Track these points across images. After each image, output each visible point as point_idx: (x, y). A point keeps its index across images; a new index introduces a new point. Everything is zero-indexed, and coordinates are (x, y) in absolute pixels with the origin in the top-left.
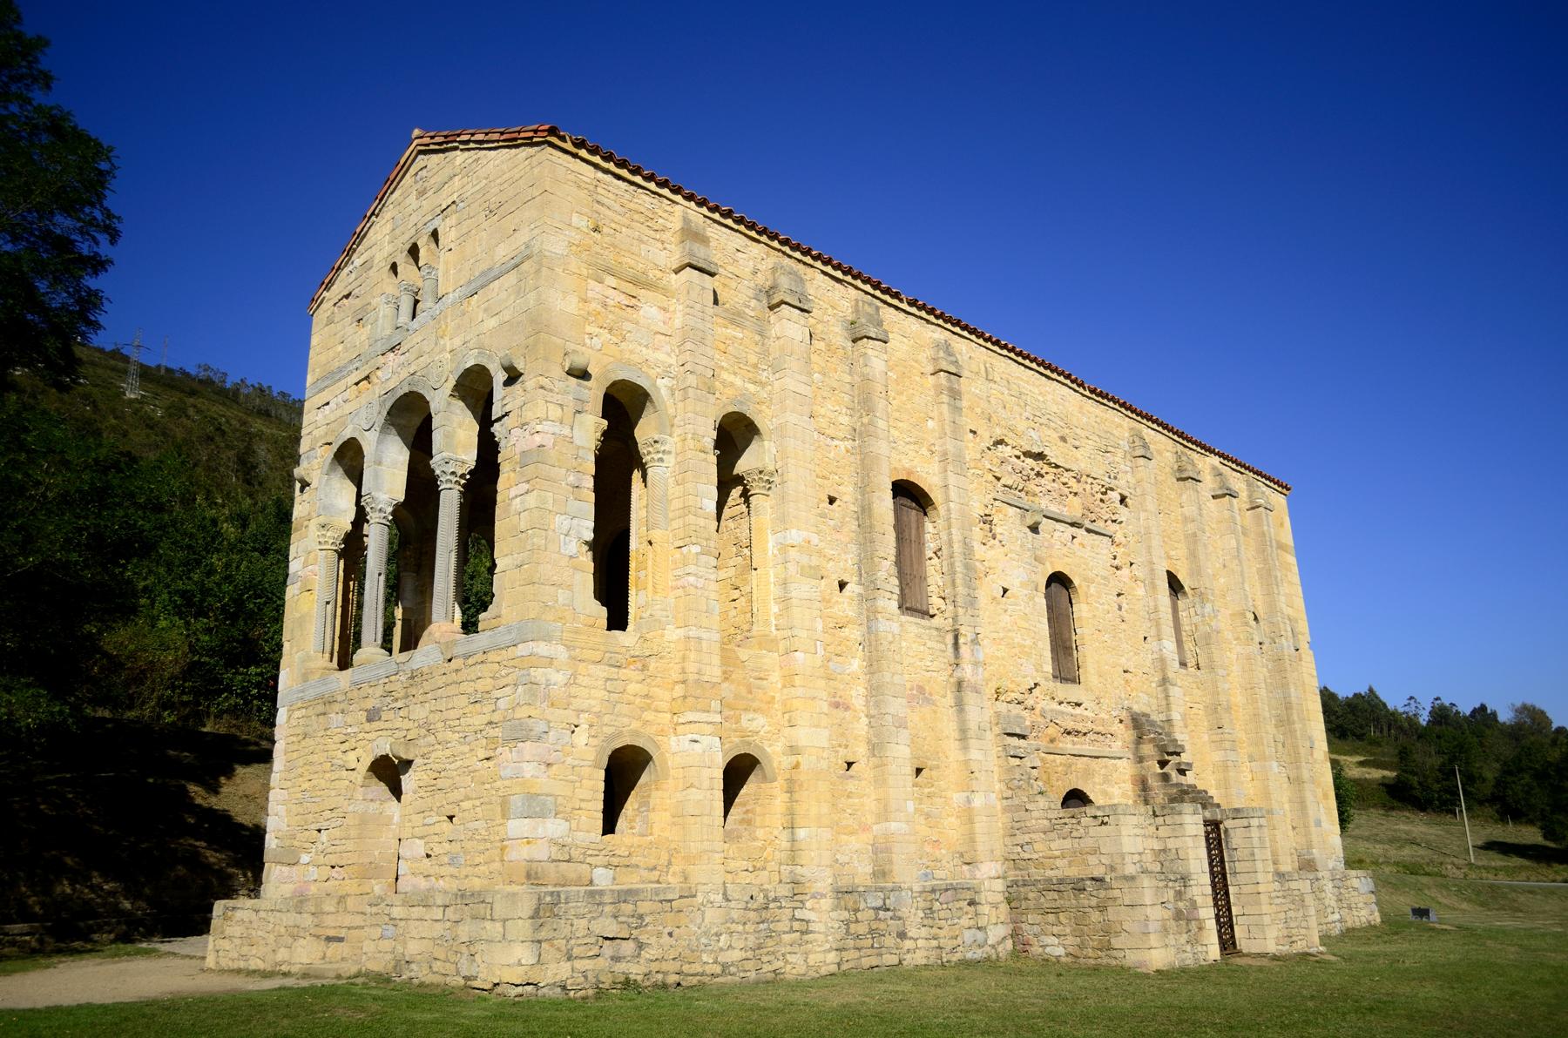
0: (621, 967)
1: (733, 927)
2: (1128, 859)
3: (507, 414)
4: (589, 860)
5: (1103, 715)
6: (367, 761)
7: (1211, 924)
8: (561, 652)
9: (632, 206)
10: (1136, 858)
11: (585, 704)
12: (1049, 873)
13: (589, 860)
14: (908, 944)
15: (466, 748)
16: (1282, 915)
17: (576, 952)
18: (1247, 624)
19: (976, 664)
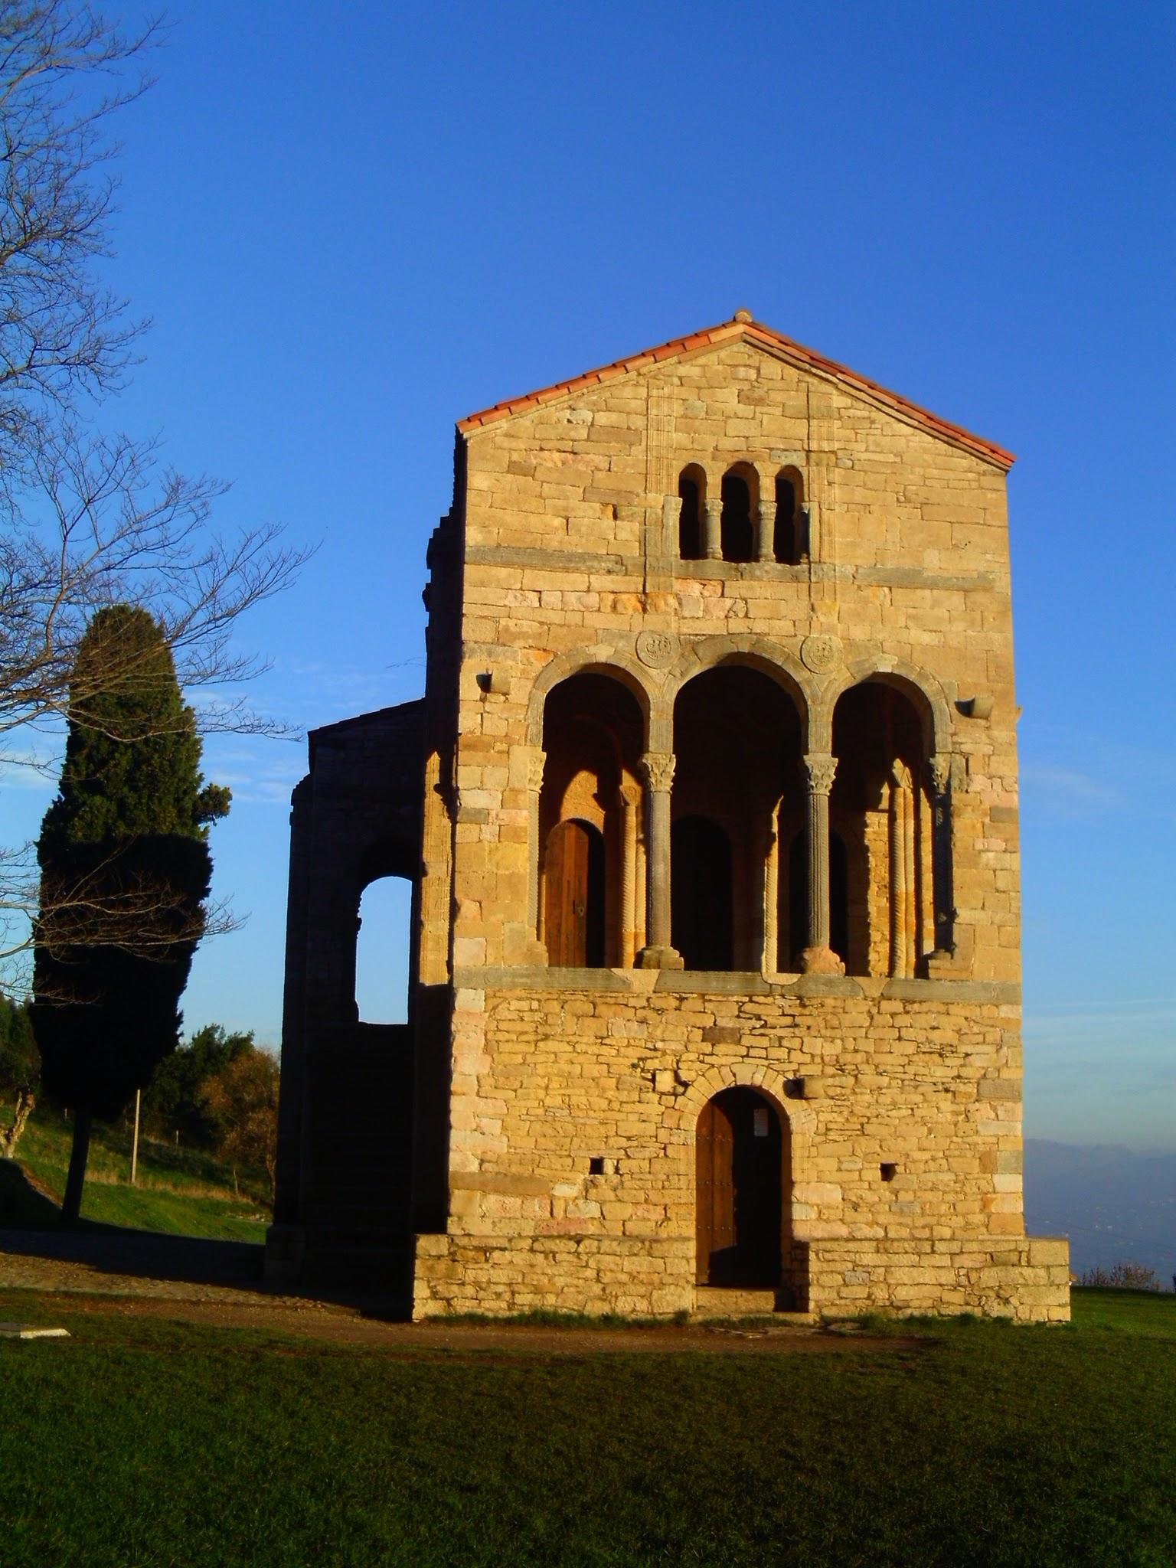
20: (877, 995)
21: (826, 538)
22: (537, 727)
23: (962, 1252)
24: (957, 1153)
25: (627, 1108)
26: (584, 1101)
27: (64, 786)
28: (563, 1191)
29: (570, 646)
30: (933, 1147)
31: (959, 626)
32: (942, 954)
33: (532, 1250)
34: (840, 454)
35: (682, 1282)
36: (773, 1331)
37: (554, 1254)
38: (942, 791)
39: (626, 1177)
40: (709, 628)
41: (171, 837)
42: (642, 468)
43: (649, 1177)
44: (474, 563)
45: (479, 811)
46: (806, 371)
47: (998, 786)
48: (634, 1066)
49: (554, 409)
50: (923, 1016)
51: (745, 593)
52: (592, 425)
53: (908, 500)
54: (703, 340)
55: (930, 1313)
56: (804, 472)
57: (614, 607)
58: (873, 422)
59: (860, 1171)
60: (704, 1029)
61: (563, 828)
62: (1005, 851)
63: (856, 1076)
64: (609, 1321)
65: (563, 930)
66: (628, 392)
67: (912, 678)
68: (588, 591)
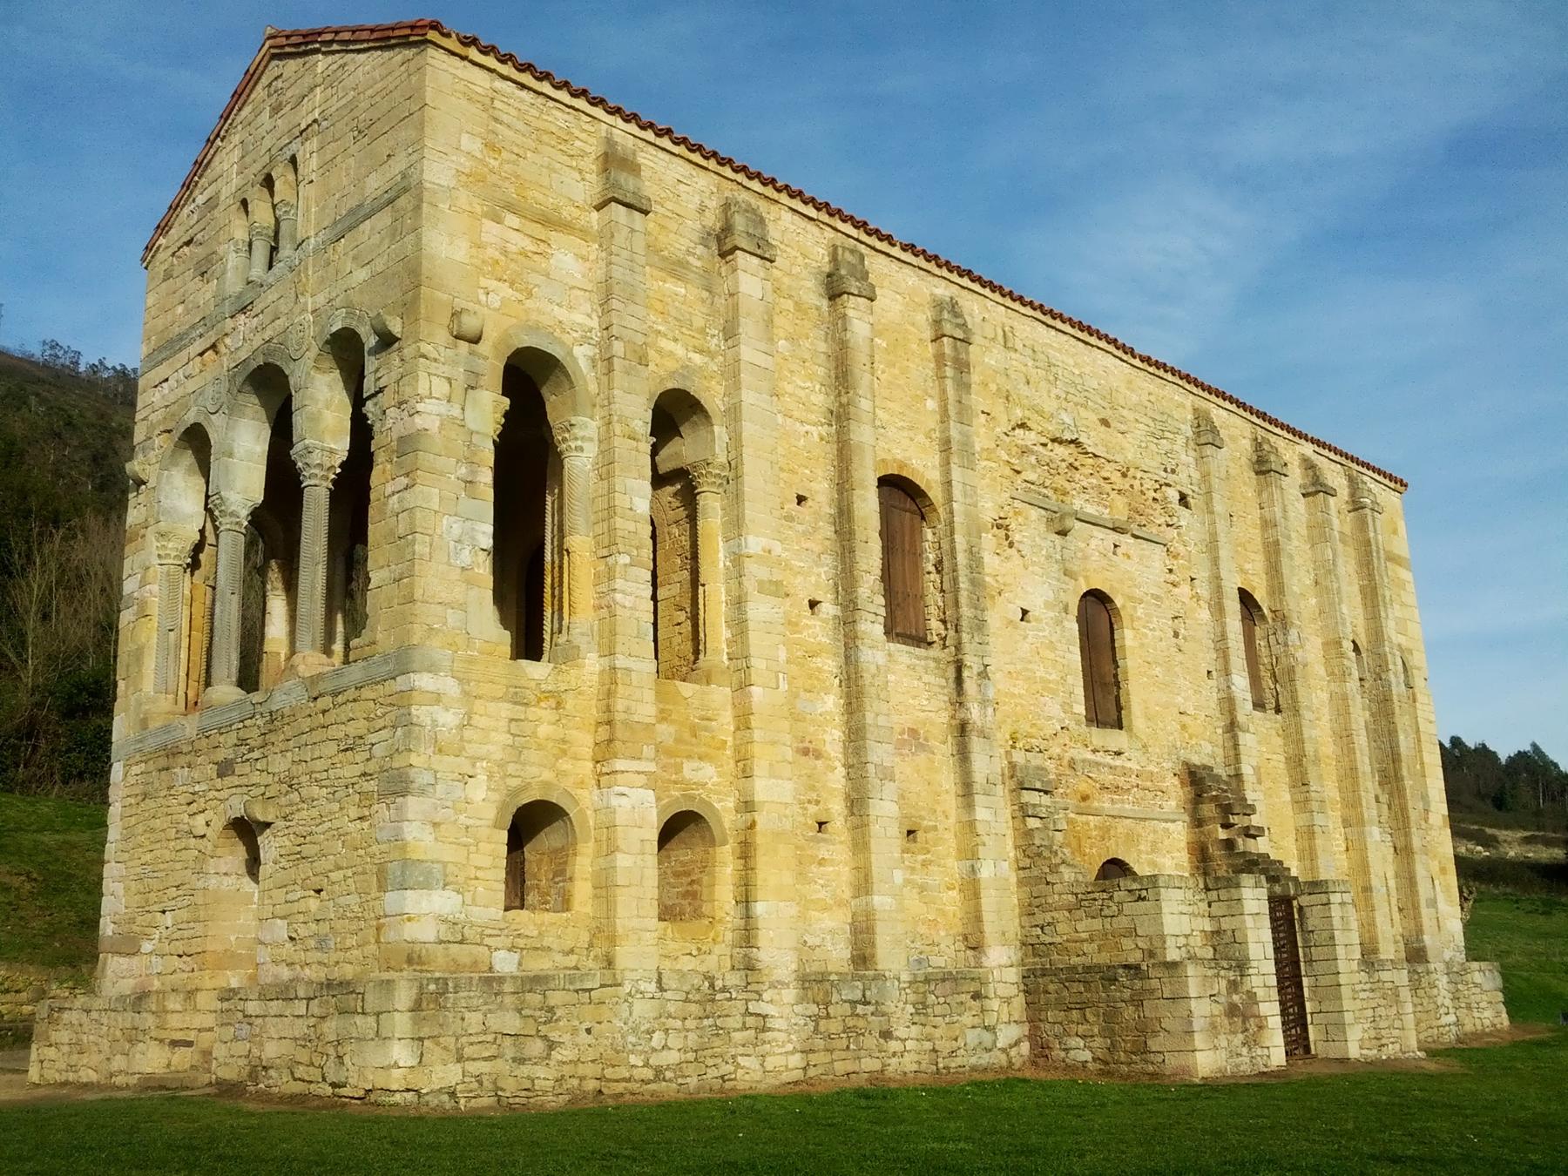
0: (525, 1070)
1: (671, 1023)
2: (1170, 942)
3: (381, 390)
4: (487, 941)
5: (1151, 768)
6: (219, 823)
7: (1275, 1022)
8: (450, 686)
9: (540, 124)
10: (1182, 941)
11: (483, 750)
12: (1075, 960)
13: (487, 941)
14: (894, 1046)
15: (336, 806)
16: (1370, 1013)
17: (468, 1051)
18: (1342, 655)
19: (984, 703)
40: (243, 355)
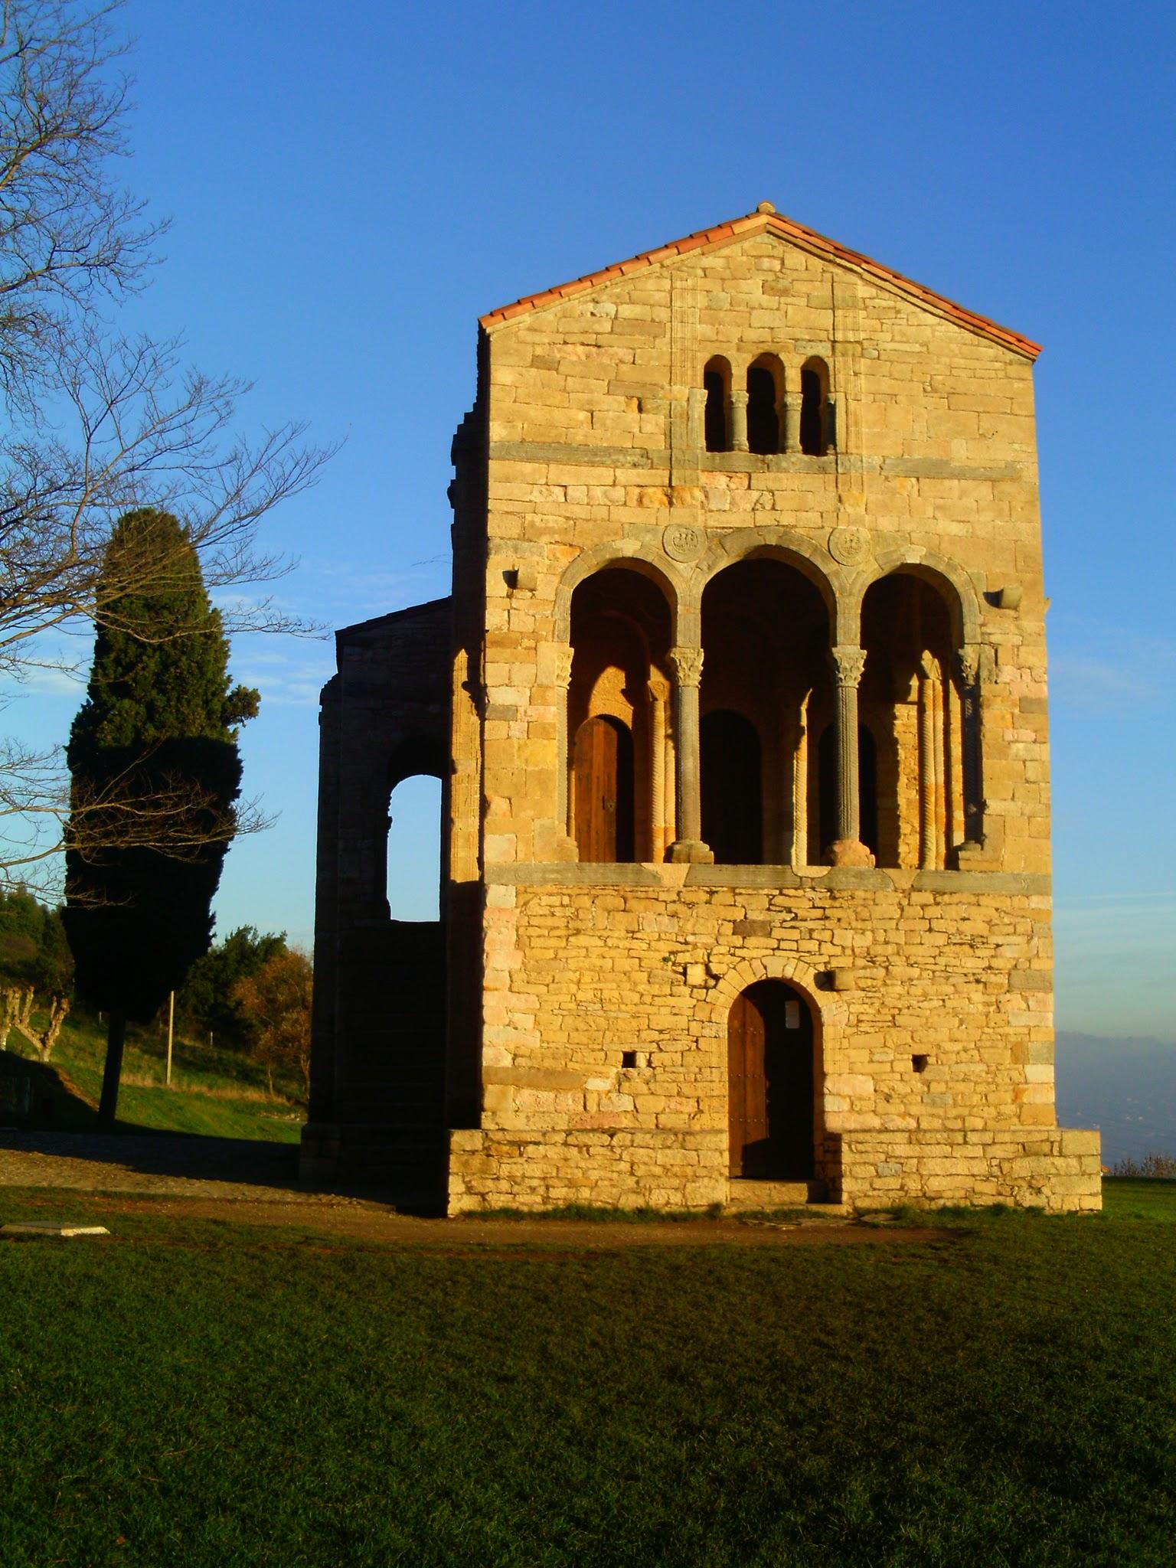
20: (907, 886)
21: (852, 429)
22: (564, 623)
23: (994, 1143)
24: (988, 1044)
25: (658, 1001)
26: (616, 995)
27: (93, 690)
28: (596, 1084)
29: (596, 540)
30: (965, 1037)
31: (987, 516)
32: (972, 845)
33: (565, 1144)
34: (866, 344)
35: (715, 1175)
36: (807, 1223)
37: (588, 1147)
38: (971, 682)
39: (659, 1070)
40: (735, 520)
41: (201, 739)
42: (666, 360)
43: (681, 1069)
44: (498, 459)
45: (507, 708)
46: (830, 261)
47: (1027, 677)
48: (665, 960)
49: (578, 301)
50: (953, 907)
51: (772, 486)
52: (616, 318)
53: (935, 390)
54: (727, 231)
55: (963, 1203)
56: (830, 362)
57: (640, 501)
58: (898, 312)
59: (892, 1062)
60: (734, 922)
61: (592, 724)
62: (1035, 742)
63: (887, 968)
64: (643, 1214)
65: (593, 825)
66: (651, 285)
67: (941, 568)
68: (614, 485)
